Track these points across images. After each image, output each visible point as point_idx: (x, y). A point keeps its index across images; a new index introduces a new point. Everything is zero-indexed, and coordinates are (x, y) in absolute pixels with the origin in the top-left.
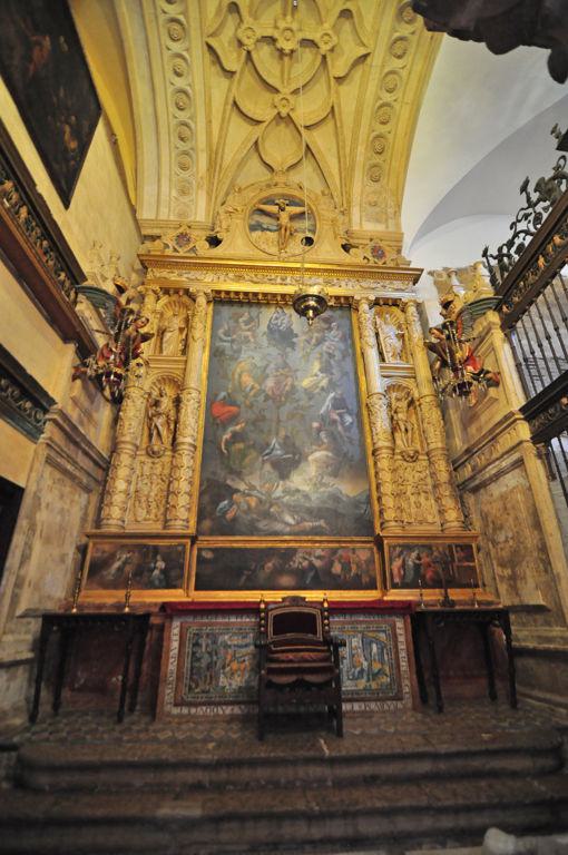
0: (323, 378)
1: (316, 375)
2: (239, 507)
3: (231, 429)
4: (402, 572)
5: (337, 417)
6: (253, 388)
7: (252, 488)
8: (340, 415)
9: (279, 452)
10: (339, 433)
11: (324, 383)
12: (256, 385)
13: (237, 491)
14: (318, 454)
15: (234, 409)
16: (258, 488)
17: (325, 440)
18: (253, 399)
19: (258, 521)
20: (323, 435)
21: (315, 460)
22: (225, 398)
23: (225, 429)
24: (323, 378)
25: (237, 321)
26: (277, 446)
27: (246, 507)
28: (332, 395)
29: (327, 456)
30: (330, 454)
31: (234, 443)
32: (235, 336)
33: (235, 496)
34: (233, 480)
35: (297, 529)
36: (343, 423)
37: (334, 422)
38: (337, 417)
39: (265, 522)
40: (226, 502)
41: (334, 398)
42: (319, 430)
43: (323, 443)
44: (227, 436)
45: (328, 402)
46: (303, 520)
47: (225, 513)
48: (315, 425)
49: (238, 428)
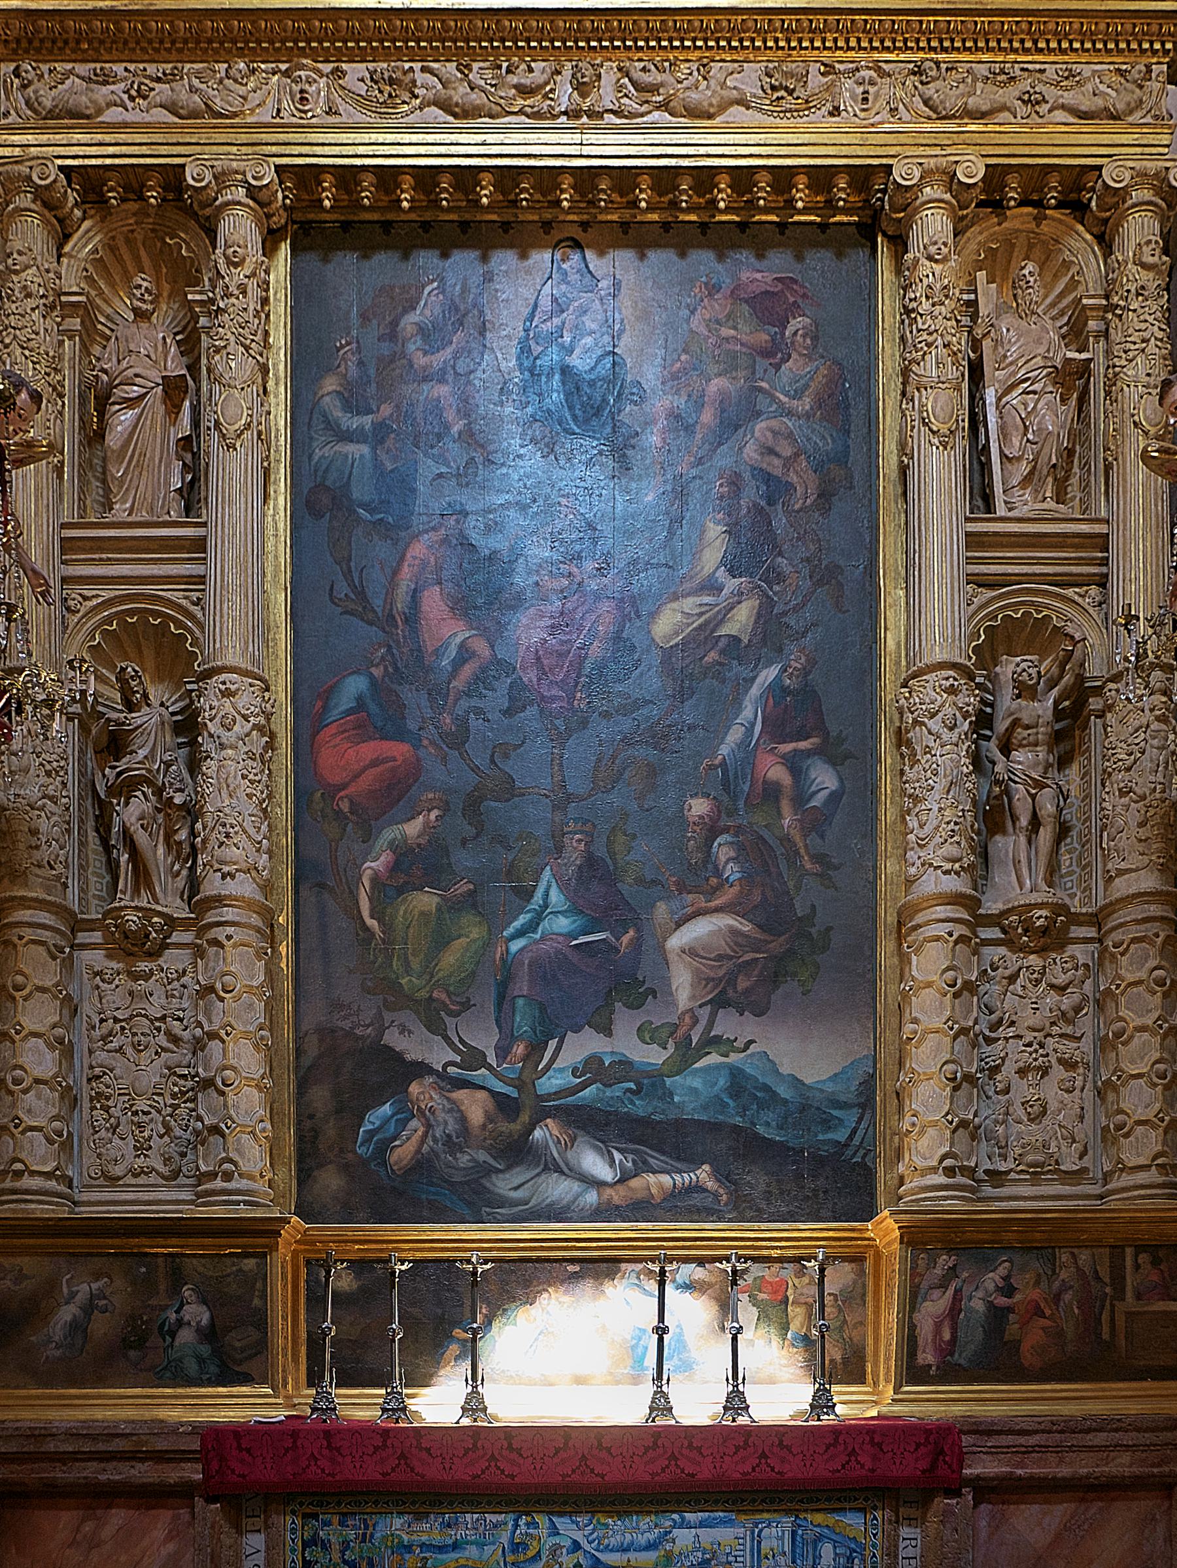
0: (739, 596)
1: (711, 586)
2: (429, 1126)
3: (390, 834)
4: (947, 1336)
5: (778, 773)
6: (465, 654)
7: (475, 1058)
8: (794, 765)
9: (563, 924)
10: (786, 840)
11: (741, 620)
12: (481, 647)
13: (421, 1069)
14: (699, 930)
15: (399, 750)
16: (492, 1060)
17: (732, 872)
18: (464, 704)
19: (490, 1171)
20: (723, 849)
21: (691, 952)
22: (360, 704)
23: (368, 836)
24: (739, 596)
25: (392, 334)
26: (555, 896)
27: (452, 1127)
28: (769, 674)
29: (734, 932)
30: (746, 927)
31: (401, 891)
32: (386, 410)
33: (414, 1088)
34: (403, 1030)
35: (617, 1196)
36: (800, 799)
37: (771, 792)
38: (778, 773)
39: (518, 1175)
40: (386, 1109)
41: (776, 690)
42: (712, 830)
43: (724, 883)
44: (377, 864)
45: (750, 710)
46: (641, 1167)
47: (384, 1147)
48: (699, 807)
49: (412, 829)
